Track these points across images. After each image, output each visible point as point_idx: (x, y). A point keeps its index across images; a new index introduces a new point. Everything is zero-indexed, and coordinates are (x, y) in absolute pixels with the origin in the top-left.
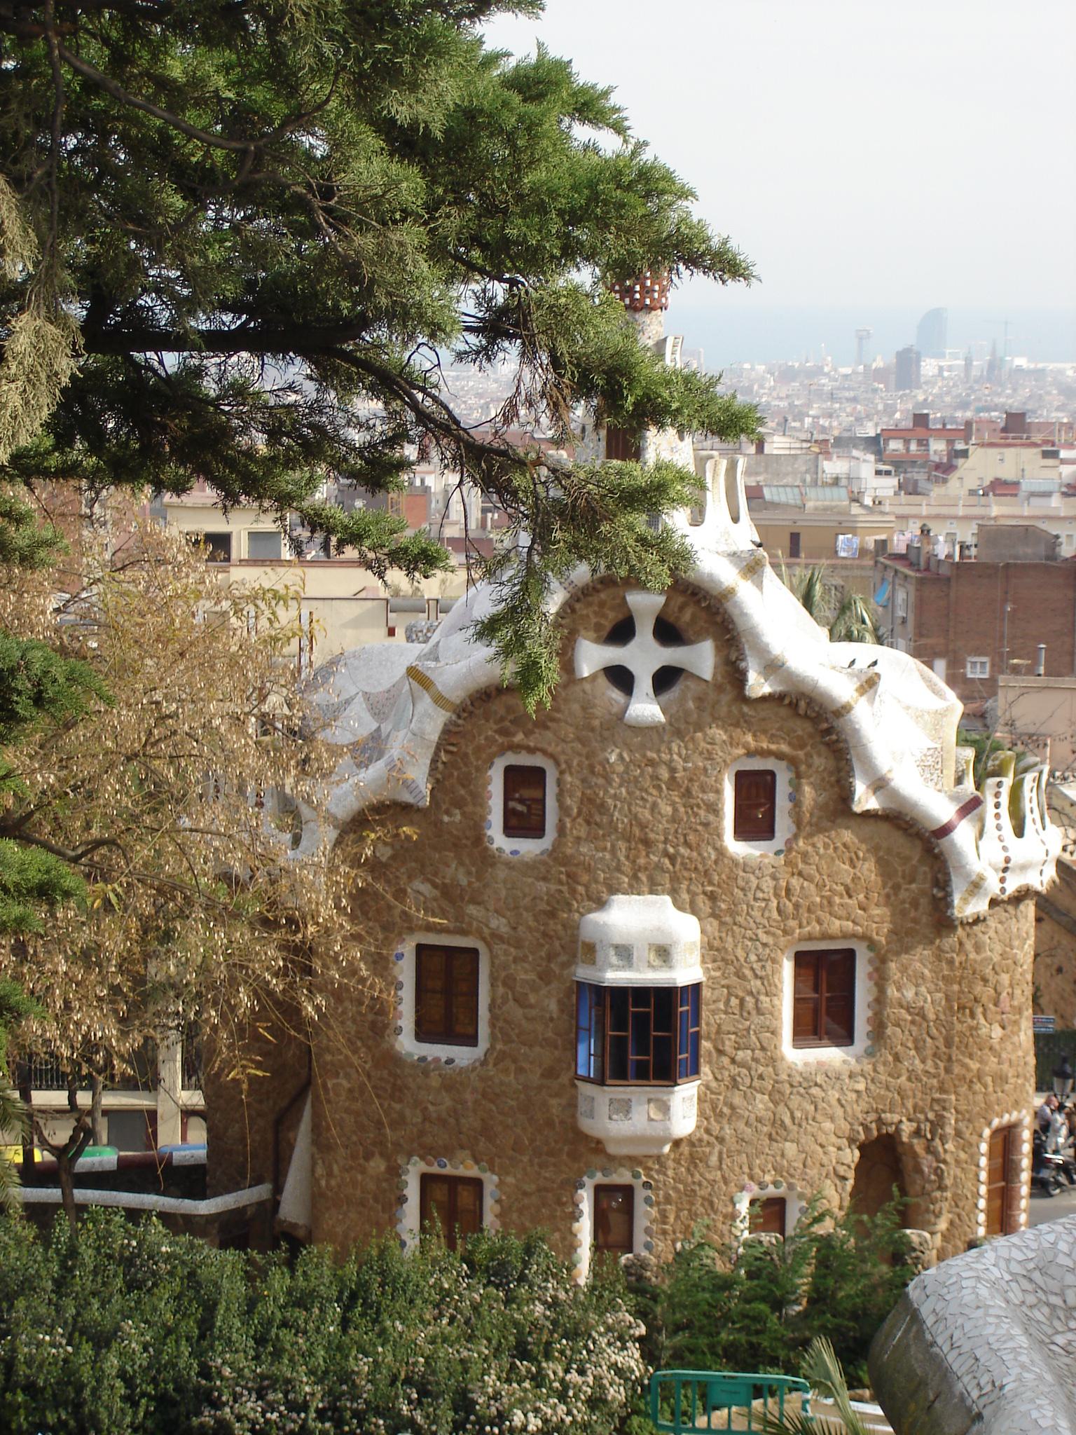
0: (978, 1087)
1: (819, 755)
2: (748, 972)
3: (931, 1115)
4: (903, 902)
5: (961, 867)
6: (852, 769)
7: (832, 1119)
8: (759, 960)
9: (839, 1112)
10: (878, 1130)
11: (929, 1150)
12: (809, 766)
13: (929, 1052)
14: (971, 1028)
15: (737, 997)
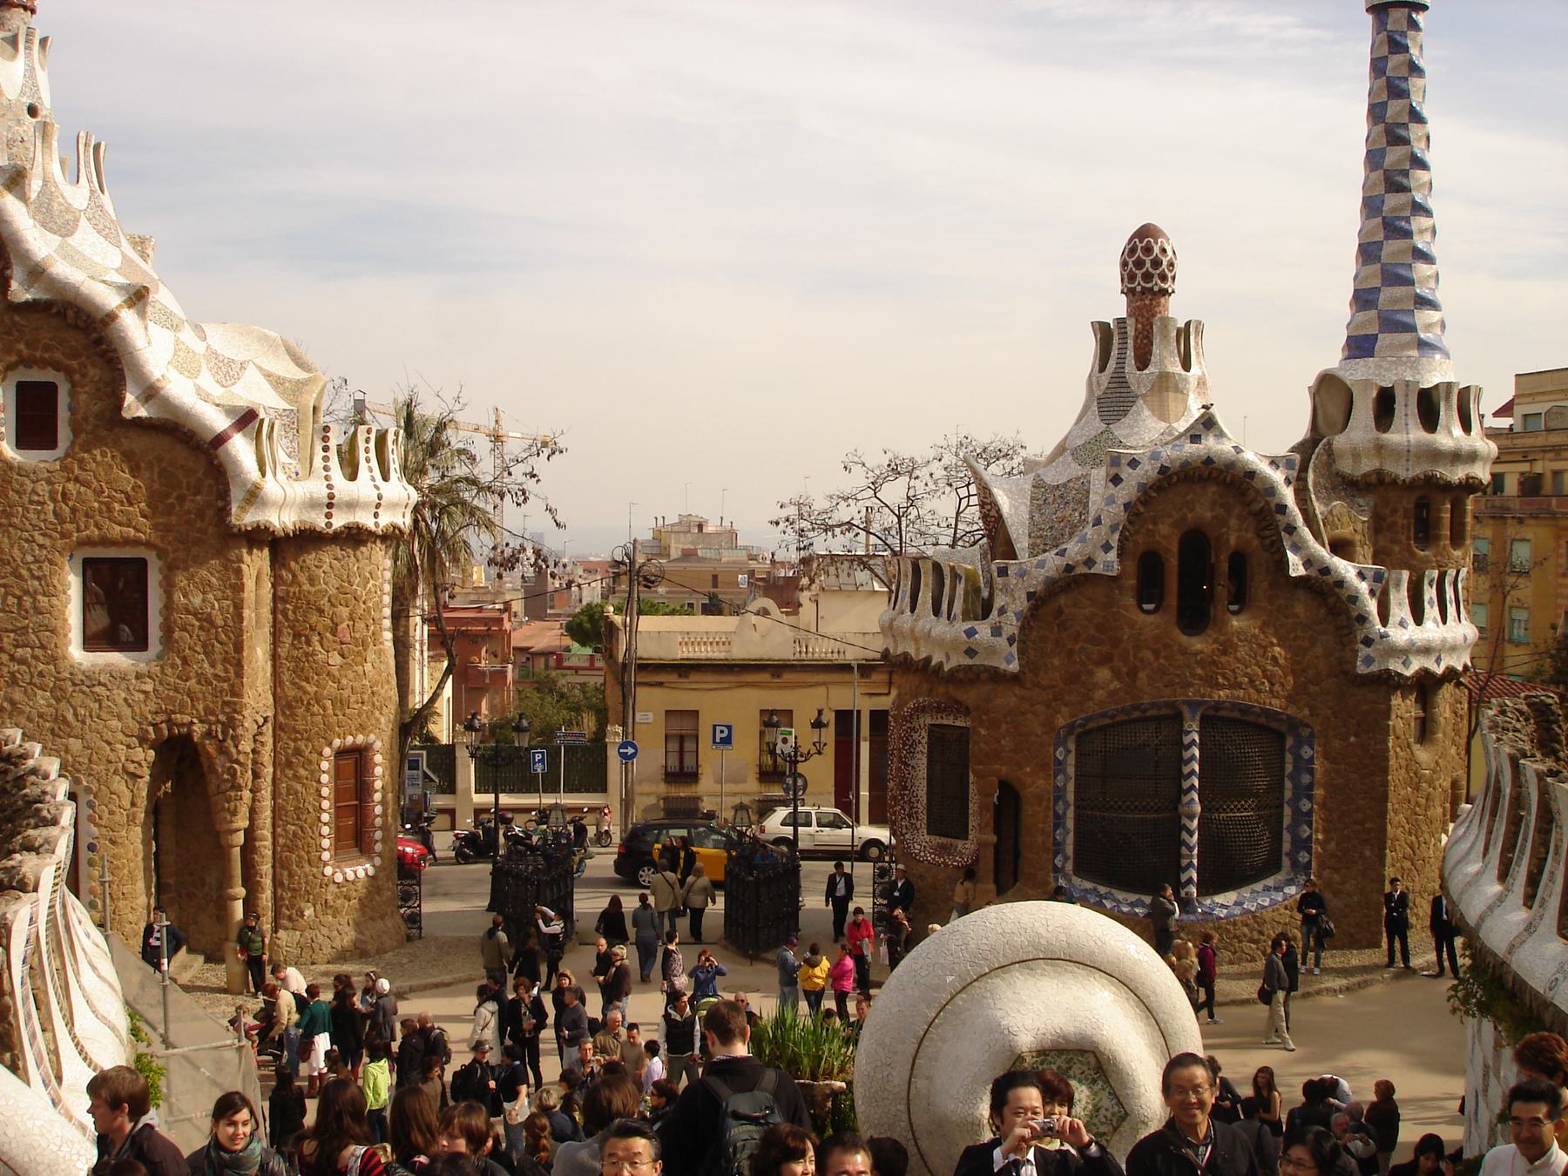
0: (316, 708)
1: (94, 366)
2: (24, 572)
3: (222, 718)
4: (189, 512)
5: (239, 474)
6: (123, 378)
7: (119, 718)
8: (36, 561)
9: (127, 711)
10: (170, 730)
11: (223, 751)
12: (84, 376)
13: (218, 657)
14: (307, 654)
15: (14, 596)
